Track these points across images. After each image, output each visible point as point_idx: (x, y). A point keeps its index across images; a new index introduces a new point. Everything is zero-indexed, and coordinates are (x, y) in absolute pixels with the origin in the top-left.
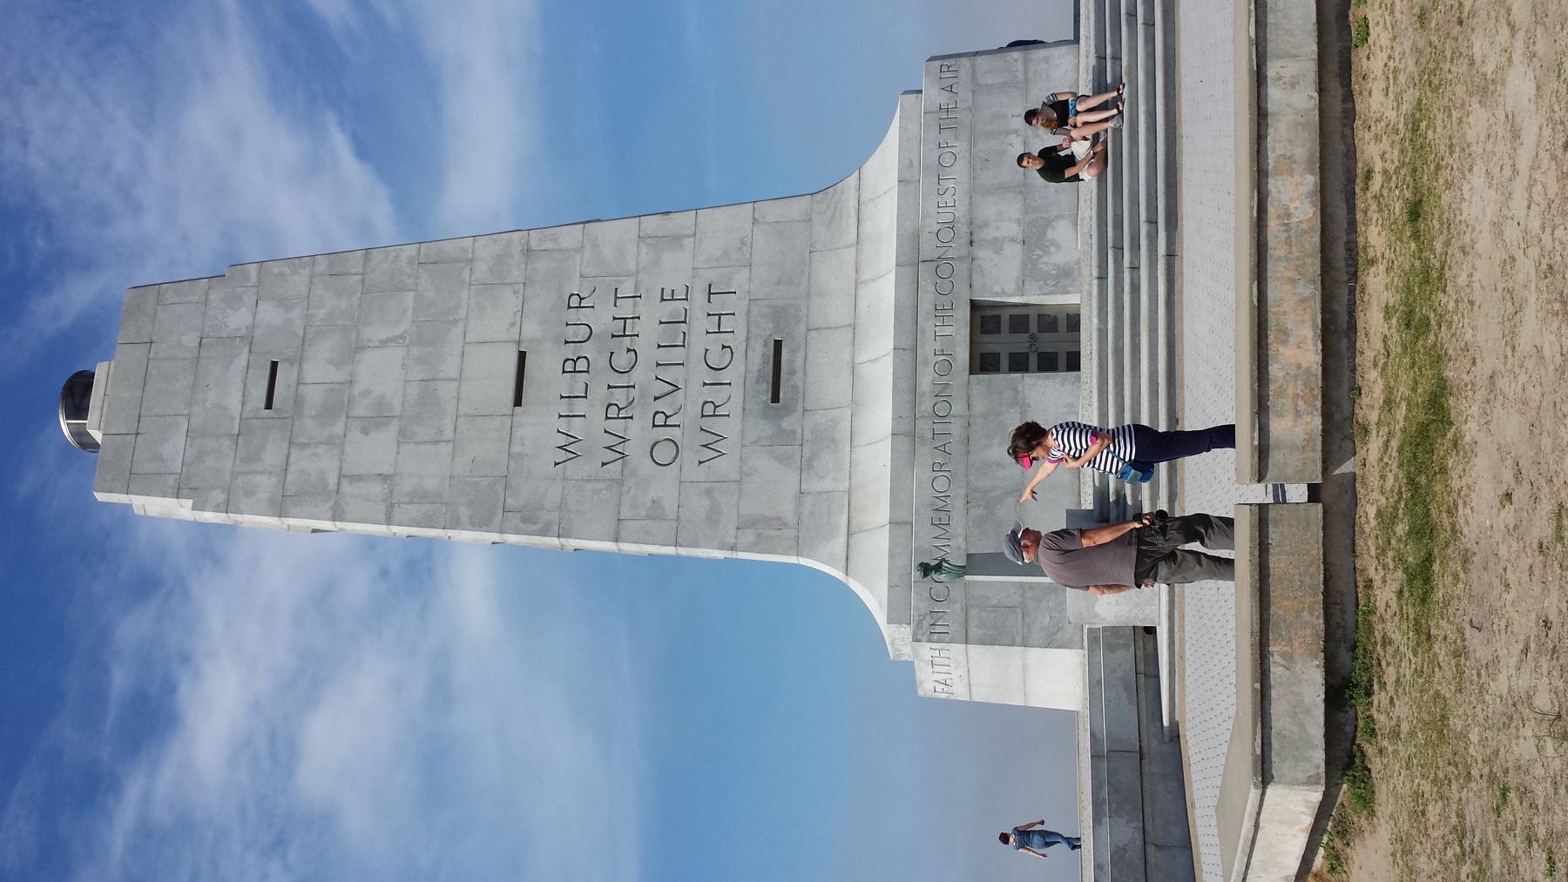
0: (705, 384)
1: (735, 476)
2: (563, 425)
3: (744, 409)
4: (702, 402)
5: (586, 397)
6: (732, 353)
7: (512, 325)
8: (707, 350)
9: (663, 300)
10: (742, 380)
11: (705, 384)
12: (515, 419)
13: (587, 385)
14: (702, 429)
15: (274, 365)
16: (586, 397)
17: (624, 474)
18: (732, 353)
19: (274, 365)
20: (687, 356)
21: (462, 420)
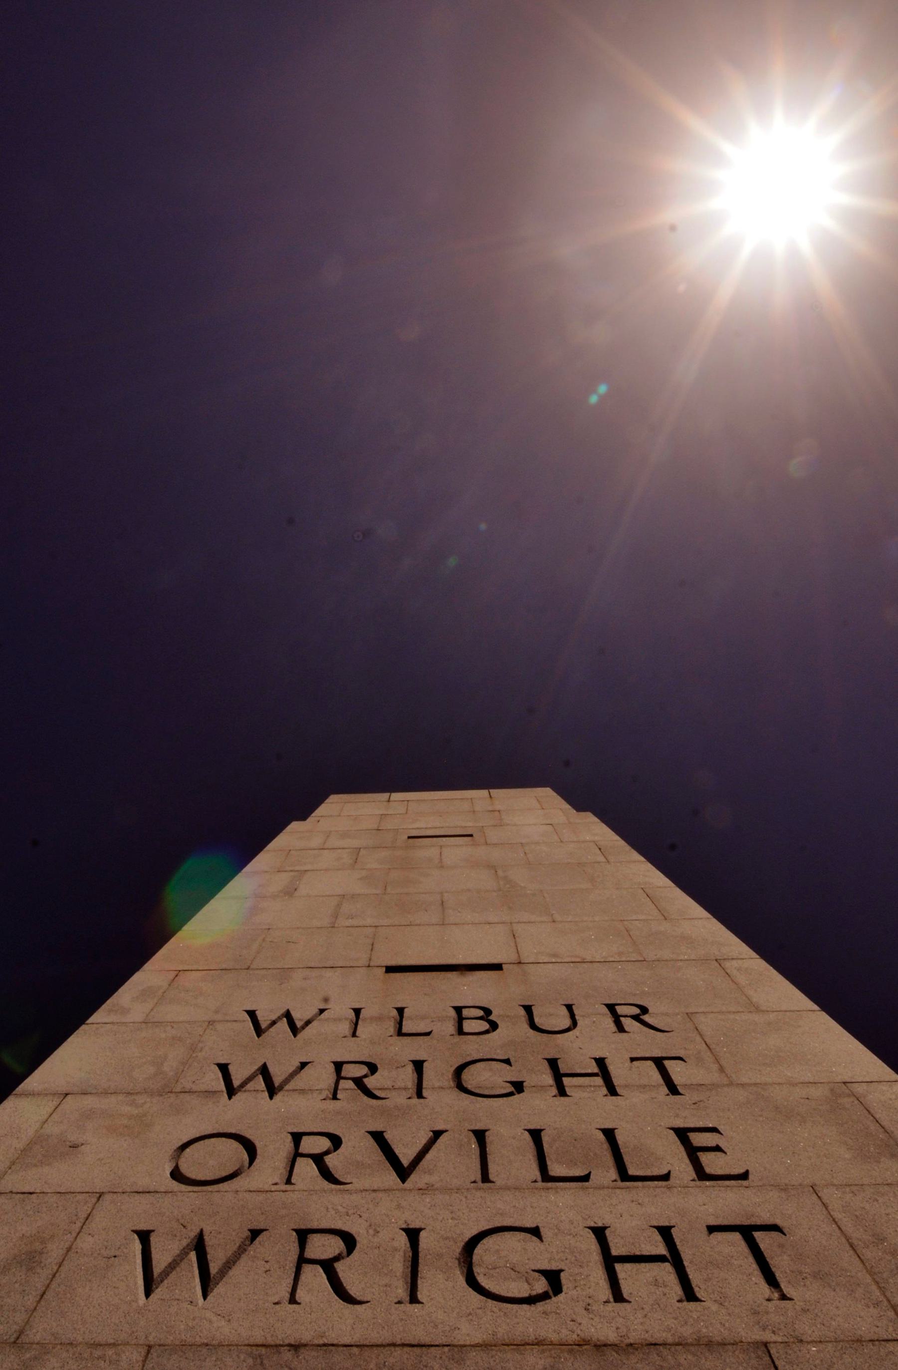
0: (413, 1234)
1: (38, 1333)
2: (341, 1009)
3: (296, 1347)
4: (353, 1231)
5: (400, 1033)
6: (531, 1300)
7: (555, 955)
8: (535, 1232)
9: (682, 1134)
10: (420, 1335)
11: (413, 1234)
12: (363, 970)
13: (428, 1034)
14: (255, 1234)
15: (471, 836)
16: (400, 1033)
17: (182, 1096)
18: (531, 1300)
19: (471, 836)
20: (507, 1188)
21: (373, 929)
